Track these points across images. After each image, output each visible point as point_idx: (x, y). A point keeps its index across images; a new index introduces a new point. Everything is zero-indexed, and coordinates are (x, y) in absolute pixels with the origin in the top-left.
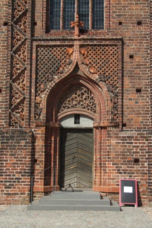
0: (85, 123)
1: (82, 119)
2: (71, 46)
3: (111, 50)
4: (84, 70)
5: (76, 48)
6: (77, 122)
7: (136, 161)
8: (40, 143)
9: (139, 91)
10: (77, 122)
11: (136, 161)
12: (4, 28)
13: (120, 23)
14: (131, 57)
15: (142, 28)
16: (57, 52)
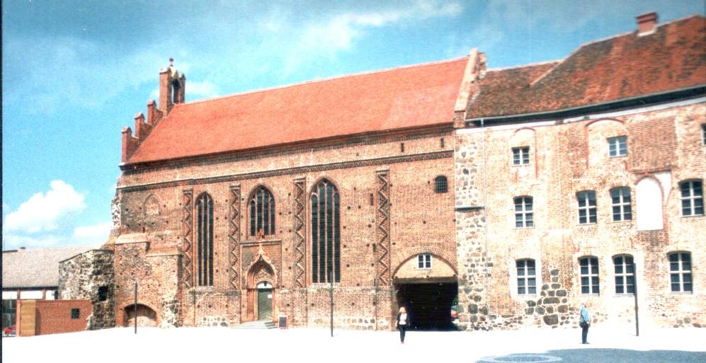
0: (269, 286)
3: (276, 247)
6: (265, 285)
7: (288, 305)
9: (290, 268)
10: (265, 285)
11: (288, 305)
13: (281, 232)
14: (287, 250)
16: (252, 249)
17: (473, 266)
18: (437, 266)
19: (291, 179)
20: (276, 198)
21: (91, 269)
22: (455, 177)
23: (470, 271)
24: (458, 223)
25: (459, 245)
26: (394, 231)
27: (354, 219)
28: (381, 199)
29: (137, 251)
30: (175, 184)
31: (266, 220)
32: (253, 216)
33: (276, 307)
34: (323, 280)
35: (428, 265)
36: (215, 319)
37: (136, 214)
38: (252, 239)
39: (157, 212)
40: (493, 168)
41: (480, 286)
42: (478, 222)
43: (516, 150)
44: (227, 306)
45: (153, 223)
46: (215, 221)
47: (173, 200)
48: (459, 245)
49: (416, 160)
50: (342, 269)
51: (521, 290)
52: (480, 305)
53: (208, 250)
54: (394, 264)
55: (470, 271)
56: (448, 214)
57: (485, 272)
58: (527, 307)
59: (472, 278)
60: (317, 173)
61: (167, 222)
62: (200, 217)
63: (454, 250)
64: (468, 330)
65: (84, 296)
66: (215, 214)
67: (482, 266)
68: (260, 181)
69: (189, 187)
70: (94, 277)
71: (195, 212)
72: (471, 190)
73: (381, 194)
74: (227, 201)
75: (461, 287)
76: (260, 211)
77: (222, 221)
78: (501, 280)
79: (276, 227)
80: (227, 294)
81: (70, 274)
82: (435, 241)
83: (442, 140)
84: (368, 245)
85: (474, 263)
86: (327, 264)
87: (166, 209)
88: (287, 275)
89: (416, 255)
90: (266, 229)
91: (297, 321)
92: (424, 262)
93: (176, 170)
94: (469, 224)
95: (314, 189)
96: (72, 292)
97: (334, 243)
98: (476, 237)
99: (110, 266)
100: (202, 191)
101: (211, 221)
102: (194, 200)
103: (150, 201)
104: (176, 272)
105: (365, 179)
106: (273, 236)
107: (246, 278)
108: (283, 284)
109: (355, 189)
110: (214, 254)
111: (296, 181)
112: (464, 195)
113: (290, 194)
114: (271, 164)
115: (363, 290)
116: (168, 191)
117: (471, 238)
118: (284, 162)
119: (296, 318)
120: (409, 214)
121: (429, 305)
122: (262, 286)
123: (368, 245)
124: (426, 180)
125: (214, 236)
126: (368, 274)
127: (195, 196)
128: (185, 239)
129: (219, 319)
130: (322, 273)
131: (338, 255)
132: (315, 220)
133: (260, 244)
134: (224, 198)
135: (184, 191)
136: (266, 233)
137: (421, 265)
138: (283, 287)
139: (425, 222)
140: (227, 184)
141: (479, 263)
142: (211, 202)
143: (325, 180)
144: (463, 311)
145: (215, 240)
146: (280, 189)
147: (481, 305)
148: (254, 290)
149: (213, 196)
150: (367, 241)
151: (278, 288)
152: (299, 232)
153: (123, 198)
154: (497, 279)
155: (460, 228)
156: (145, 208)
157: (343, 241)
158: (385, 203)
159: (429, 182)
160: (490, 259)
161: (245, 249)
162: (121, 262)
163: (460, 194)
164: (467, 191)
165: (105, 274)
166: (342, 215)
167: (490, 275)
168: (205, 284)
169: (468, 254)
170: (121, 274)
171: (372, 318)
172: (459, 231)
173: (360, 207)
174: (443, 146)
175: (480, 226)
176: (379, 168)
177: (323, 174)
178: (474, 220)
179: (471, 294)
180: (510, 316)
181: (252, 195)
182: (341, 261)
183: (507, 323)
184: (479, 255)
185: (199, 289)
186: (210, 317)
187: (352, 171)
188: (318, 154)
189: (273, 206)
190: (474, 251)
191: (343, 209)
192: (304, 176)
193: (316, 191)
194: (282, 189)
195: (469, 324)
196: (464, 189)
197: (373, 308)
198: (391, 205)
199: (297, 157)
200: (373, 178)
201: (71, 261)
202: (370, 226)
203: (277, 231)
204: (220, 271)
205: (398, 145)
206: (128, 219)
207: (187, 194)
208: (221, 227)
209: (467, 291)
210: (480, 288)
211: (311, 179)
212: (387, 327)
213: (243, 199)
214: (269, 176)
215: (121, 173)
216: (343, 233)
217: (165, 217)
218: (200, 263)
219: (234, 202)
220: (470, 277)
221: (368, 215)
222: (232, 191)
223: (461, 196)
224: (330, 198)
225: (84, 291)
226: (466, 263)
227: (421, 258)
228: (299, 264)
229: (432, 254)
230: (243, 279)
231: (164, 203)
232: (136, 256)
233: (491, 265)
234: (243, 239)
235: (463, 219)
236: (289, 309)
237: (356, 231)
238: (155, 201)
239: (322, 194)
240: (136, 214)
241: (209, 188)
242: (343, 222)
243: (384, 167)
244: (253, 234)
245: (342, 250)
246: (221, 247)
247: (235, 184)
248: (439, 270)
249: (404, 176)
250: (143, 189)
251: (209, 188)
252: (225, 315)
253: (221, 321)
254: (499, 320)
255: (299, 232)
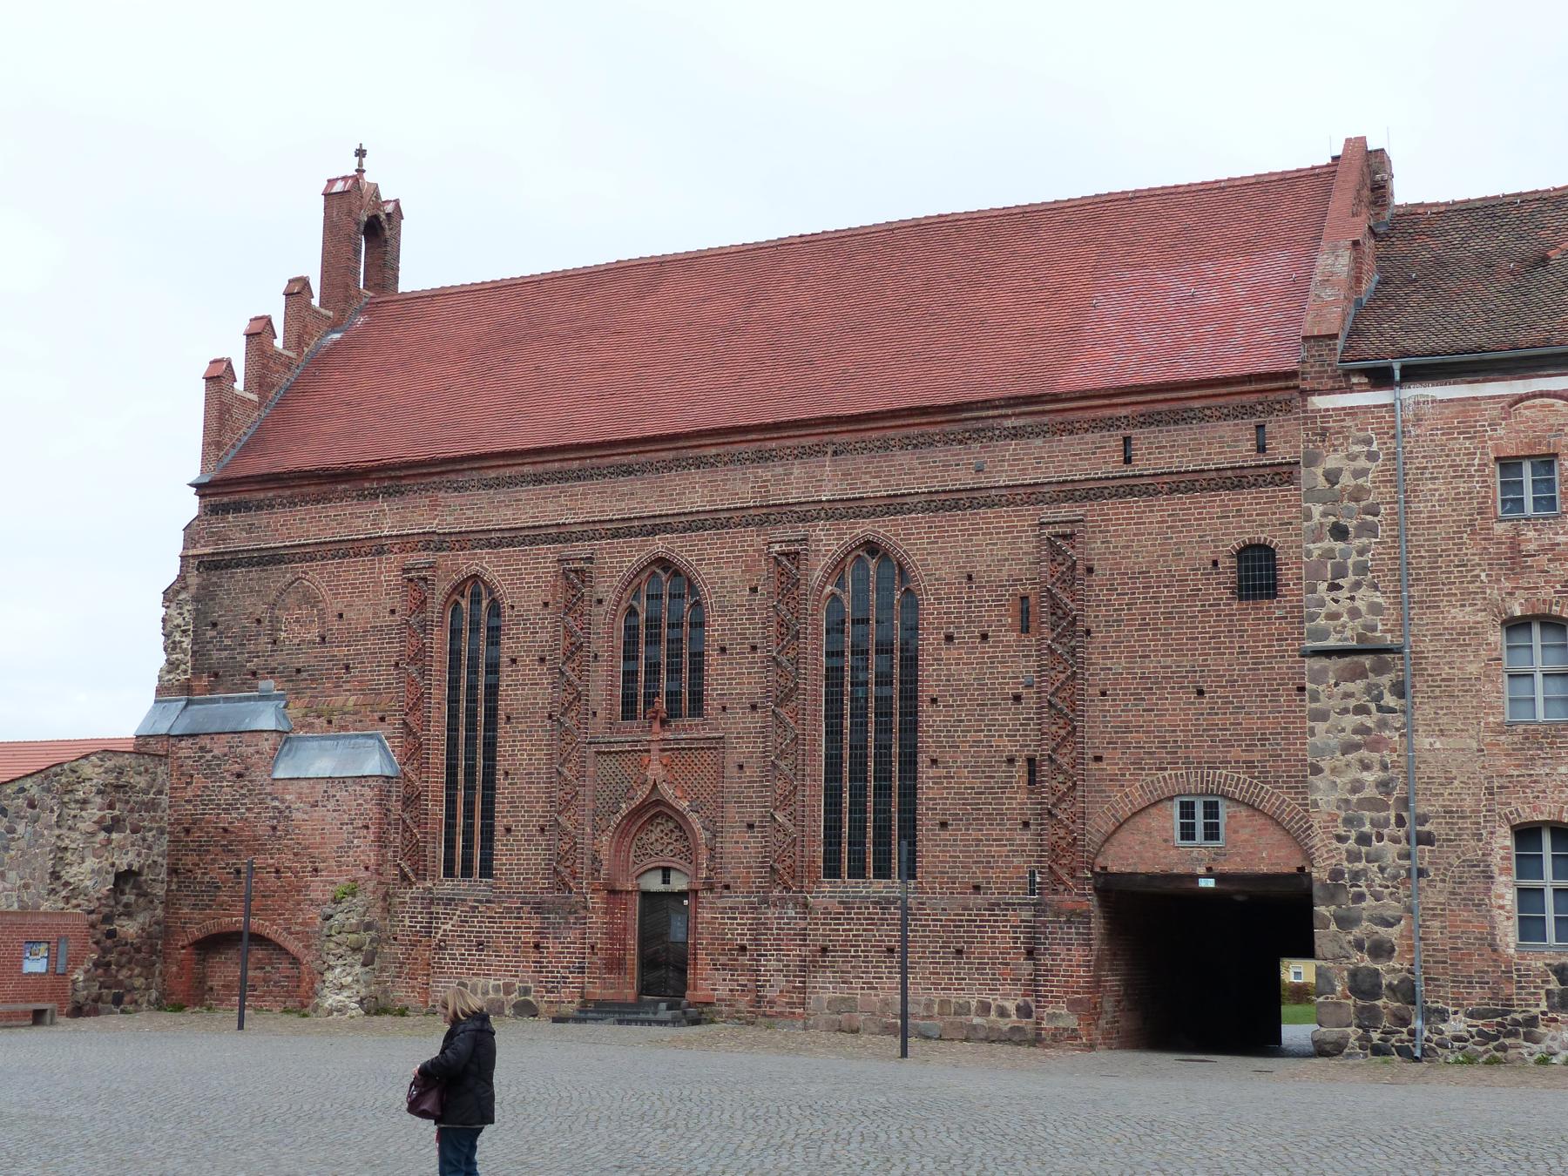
0: (678, 883)
1: (672, 874)
2: (648, 751)
3: (709, 757)
4: (668, 792)
5: (655, 755)
6: (666, 881)
8: (597, 920)
9: (751, 826)
10: (666, 881)
11: (743, 948)
12: (548, 722)
13: (724, 709)
14: (741, 767)
15: (758, 715)
17: (1364, 839)
18: (1244, 834)
19: (759, 541)
20: (710, 601)
21: (94, 812)
22: (1303, 550)
23: (1353, 857)
24: (1315, 698)
25: (1316, 770)
26: (1100, 719)
27: (967, 675)
28: (1055, 610)
29: (243, 758)
30: (377, 548)
31: (674, 671)
32: (630, 656)
33: (701, 955)
34: (858, 871)
35: (1212, 833)
36: (497, 989)
37: (244, 638)
38: (634, 731)
39: (314, 633)
40: (1432, 520)
41: (1391, 907)
42: (1380, 696)
43: (1508, 465)
44: (537, 946)
45: (298, 671)
46: (505, 669)
47: (367, 598)
48: (1316, 770)
49: (1171, 491)
50: (922, 833)
51: (1530, 928)
52: (1389, 971)
53: (480, 763)
54: (1099, 823)
55: (1353, 857)
56: (1282, 667)
57: (1406, 863)
58: (1554, 985)
59: (1362, 883)
60: (844, 525)
61: (347, 667)
62: (455, 654)
63: (1300, 786)
64: (1350, 1055)
65: (67, 899)
66: (507, 646)
67: (1396, 840)
68: (659, 545)
69: (423, 558)
70: (102, 835)
71: (439, 640)
72: (1358, 595)
73: (1052, 596)
74: (546, 604)
75: (1321, 909)
76: (653, 640)
77: (528, 667)
78: (1463, 890)
79: (708, 690)
80: (539, 908)
81: (21, 828)
82: (1236, 753)
83: (1260, 427)
84: (1011, 761)
85: (1367, 828)
86: (871, 814)
87: (343, 625)
88: (742, 851)
89: (1171, 798)
90: (674, 697)
91: (772, 1003)
92: (1200, 821)
93: (382, 504)
94: (1352, 703)
95: (837, 570)
96: (26, 886)
97: (896, 750)
98: (1375, 746)
99: (152, 806)
100: (465, 572)
101: (493, 668)
102: (439, 598)
103: (291, 600)
104: (373, 828)
105: (1003, 548)
106: (698, 720)
107: (605, 854)
108: (727, 880)
109: (970, 578)
110: (500, 776)
111: (777, 548)
112: (1333, 607)
113: (754, 590)
114: (695, 492)
115: (992, 907)
116: (355, 570)
117: (1356, 747)
118: (738, 487)
119: (769, 993)
120: (1150, 664)
121: (1204, 968)
122: (654, 883)
123: (1011, 761)
124: (1207, 554)
125: (502, 714)
126: (1010, 853)
127: (443, 587)
128: (405, 723)
129: (508, 989)
130: (857, 842)
131: (910, 793)
132: (834, 676)
133: (654, 747)
134: (539, 596)
135: (405, 571)
136: (674, 712)
137: (1187, 833)
138: (727, 887)
139: (1201, 693)
140: (549, 552)
141: (1386, 831)
142: (495, 609)
143: (871, 547)
144: (1333, 991)
145: (503, 727)
146: (726, 572)
147: (1394, 970)
148: (628, 892)
149: (503, 589)
150: (1010, 748)
151: (711, 889)
152: (781, 711)
153: (201, 587)
154: (1449, 886)
155: (1322, 716)
156: (275, 620)
157: (928, 744)
158: (1069, 625)
159: (1215, 563)
160: (1422, 819)
161: (611, 762)
162: (189, 794)
163: (1321, 603)
164: (1342, 595)
165: (134, 831)
166: (924, 659)
167: (1422, 873)
168: (467, 871)
169: (1347, 801)
170: (187, 831)
171: (1020, 1000)
172: (1320, 727)
173: (984, 637)
174: (1261, 449)
175: (1392, 711)
176: (1048, 513)
177: (865, 528)
178: (1368, 690)
179: (1357, 932)
180: (1496, 1014)
181: (631, 583)
182: (921, 809)
183: (1486, 1038)
184: (1387, 807)
185: (447, 887)
186: (481, 981)
187: (962, 521)
188: (848, 462)
189: (698, 624)
190: (1370, 792)
191: (929, 642)
192: (802, 530)
193: (840, 584)
194: (727, 573)
195: (1353, 1032)
196: (1334, 587)
197: (1026, 967)
198: (1088, 632)
199: (780, 470)
200: (1027, 544)
201: (28, 783)
202: (1017, 698)
203: (711, 704)
204: (519, 832)
205: (1113, 440)
206: (215, 655)
207: (416, 582)
208: (525, 690)
209: (1345, 922)
210: (1388, 913)
211: (828, 543)
212: (1073, 1035)
213: (600, 601)
214: (689, 528)
215: (191, 506)
216: (930, 718)
217: (341, 652)
218: (451, 802)
219: (569, 609)
220: (1356, 876)
221: (1016, 662)
222: (565, 574)
223: (1323, 611)
224: (885, 605)
225: (67, 884)
226: (1341, 831)
227: (1187, 810)
228: (779, 817)
229: (1224, 796)
230: (595, 859)
231: (339, 606)
232: (239, 775)
233: (1426, 839)
234: (598, 727)
235: (1332, 689)
236: (745, 959)
237: (970, 713)
238: (310, 600)
239: (860, 595)
240: (244, 638)
241: (487, 564)
242: (930, 679)
243: (1065, 511)
244: (629, 711)
245: (925, 772)
246: (522, 752)
247: (581, 549)
248: (1251, 850)
249: (1126, 538)
250: (270, 559)
251: (487, 564)
252: (526, 978)
253: (515, 997)
254: (1457, 1025)
255: (781, 711)
